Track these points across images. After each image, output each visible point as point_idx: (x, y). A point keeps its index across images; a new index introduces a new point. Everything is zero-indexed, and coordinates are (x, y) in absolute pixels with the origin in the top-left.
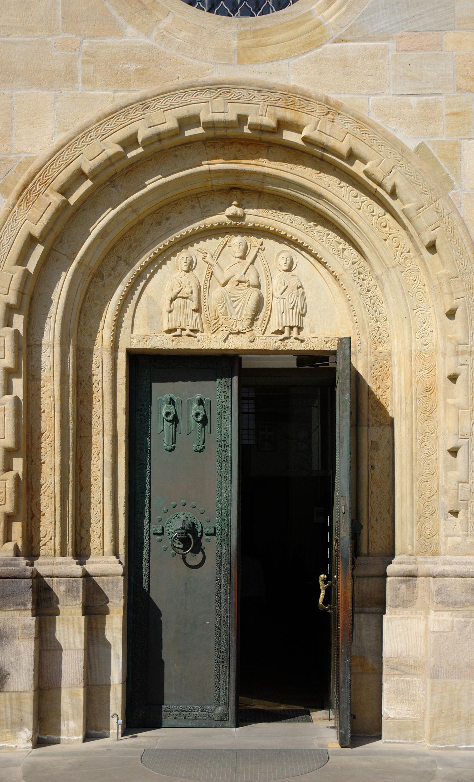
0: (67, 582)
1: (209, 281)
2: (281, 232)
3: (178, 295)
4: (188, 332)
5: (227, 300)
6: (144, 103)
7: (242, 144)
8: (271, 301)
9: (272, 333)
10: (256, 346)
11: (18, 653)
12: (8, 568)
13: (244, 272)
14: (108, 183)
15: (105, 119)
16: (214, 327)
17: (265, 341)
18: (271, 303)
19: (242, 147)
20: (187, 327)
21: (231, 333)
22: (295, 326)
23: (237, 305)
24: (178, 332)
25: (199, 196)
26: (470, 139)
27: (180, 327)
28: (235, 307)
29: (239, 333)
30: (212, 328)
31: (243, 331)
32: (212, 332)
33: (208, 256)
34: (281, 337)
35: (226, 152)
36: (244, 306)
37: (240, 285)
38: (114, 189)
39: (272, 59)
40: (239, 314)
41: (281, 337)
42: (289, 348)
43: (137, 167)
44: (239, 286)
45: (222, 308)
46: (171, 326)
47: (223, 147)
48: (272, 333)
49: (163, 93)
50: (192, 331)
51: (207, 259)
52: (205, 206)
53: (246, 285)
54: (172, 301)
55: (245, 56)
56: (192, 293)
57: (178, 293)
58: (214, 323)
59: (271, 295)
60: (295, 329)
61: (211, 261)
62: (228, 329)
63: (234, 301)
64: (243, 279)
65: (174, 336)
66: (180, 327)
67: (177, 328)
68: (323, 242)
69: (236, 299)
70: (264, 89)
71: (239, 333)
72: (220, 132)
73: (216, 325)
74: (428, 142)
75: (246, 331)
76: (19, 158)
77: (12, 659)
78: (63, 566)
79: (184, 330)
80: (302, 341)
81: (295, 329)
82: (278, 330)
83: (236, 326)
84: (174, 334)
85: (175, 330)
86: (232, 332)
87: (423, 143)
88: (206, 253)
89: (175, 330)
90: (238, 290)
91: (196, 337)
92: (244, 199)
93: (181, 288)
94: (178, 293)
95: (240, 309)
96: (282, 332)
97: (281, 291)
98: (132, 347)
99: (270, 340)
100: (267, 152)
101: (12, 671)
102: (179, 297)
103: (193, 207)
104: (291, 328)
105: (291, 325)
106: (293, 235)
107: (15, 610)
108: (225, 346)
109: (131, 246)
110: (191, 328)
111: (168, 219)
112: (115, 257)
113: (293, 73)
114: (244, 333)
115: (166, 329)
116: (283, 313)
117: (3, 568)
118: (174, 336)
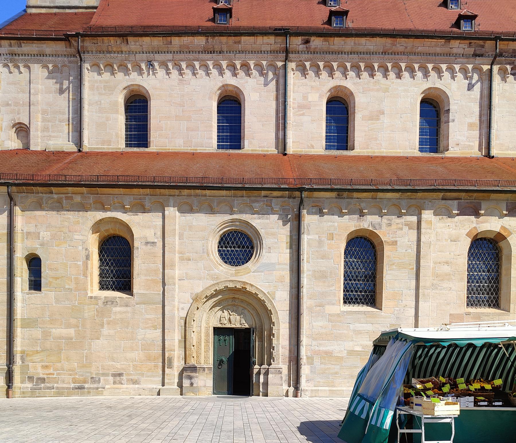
55: (236, 274)
70: (239, 282)
113: (245, 278)
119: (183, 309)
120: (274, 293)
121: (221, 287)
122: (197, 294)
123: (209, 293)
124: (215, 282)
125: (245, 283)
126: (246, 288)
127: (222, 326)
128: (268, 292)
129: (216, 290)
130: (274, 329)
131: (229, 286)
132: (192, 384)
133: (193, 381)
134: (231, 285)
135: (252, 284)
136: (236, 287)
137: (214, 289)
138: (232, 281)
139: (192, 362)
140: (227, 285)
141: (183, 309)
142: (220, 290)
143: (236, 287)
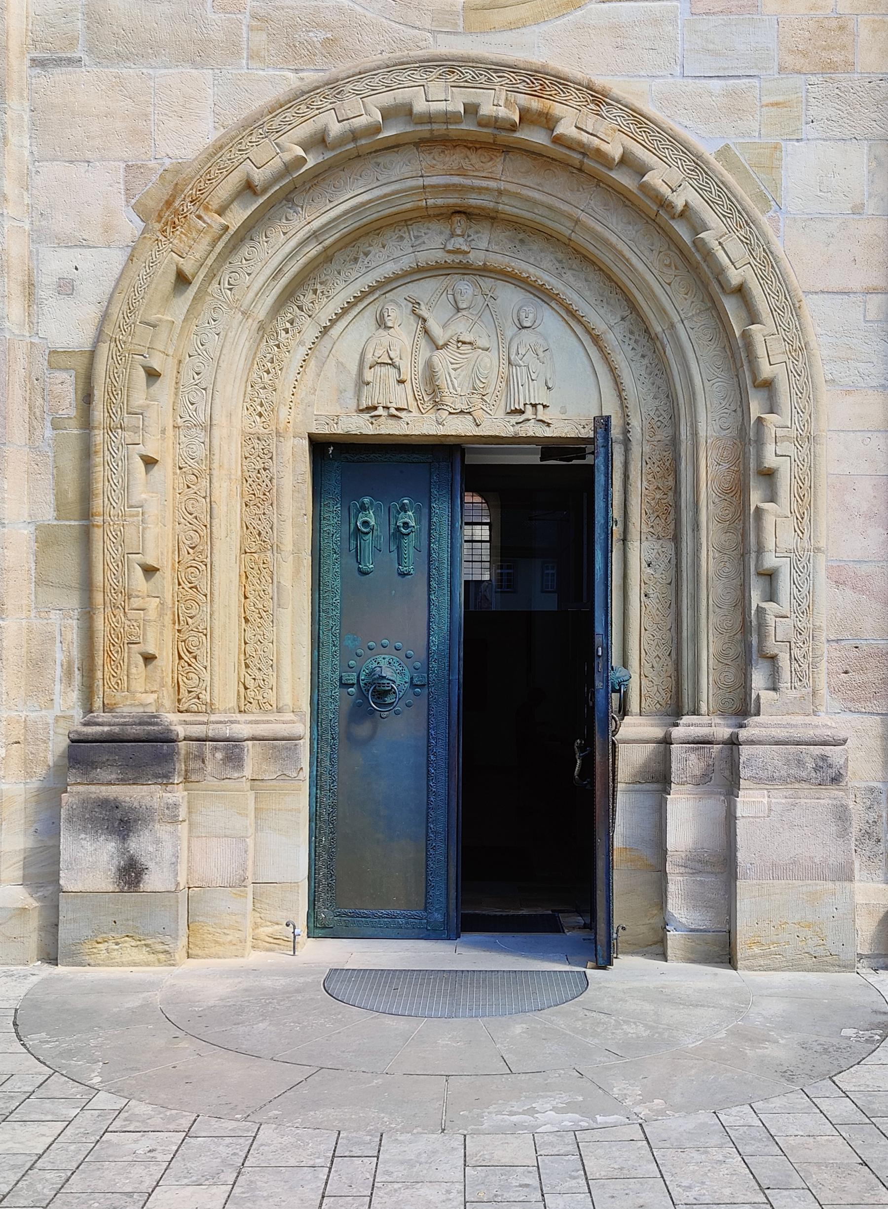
0: (226, 748)
6: (334, 87)
7: (469, 148)
10: (486, 430)
11: (158, 841)
12: (145, 727)
14: (284, 202)
15: (280, 110)
19: (469, 153)
20: (389, 405)
24: (380, 411)
25: (409, 223)
26: (798, 140)
35: (447, 159)
38: (292, 211)
39: (512, 26)
42: (531, 434)
43: (324, 179)
47: (443, 152)
49: (360, 73)
50: (397, 409)
52: (417, 237)
59: (506, 362)
60: (540, 407)
62: (446, 408)
69: (458, 366)
70: (499, 68)
72: (439, 128)
74: (734, 144)
76: (162, 165)
77: (151, 849)
78: (220, 726)
80: (548, 425)
81: (540, 407)
84: (372, 414)
87: (727, 146)
89: (375, 408)
92: (471, 227)
98: (317, 432)
100: (504, 160)
101: (151, 865)
103: (402, 238)
104: (534, 406)
107: (156, 783)
108: (442, 431)
109: (315, 292)
111: (366, 254)
112: (295, 307)
117: (138, 728)
118: (372, 417)
119: (66, 287)
120: (771, 160)
121: (363, 111)
122: (178, 169)
123: (265, 160)
124: (311, 77)
125: (542, 80)
126: (547, 121)
127: (370, 430)
128: (724, 153)
129: (319, 141)
130: (771, 431)
131: (420, 106)
132: (131, 873)
133: (141, 844)
134: (437, 97)
135: (600, 81)
136: (471, 109)
137: (305, 130)
138: (448, 66)
139: (142, 696)
140: (401, 95)
141: (66, 287)
142: (354, 135)
143: (471, 109)
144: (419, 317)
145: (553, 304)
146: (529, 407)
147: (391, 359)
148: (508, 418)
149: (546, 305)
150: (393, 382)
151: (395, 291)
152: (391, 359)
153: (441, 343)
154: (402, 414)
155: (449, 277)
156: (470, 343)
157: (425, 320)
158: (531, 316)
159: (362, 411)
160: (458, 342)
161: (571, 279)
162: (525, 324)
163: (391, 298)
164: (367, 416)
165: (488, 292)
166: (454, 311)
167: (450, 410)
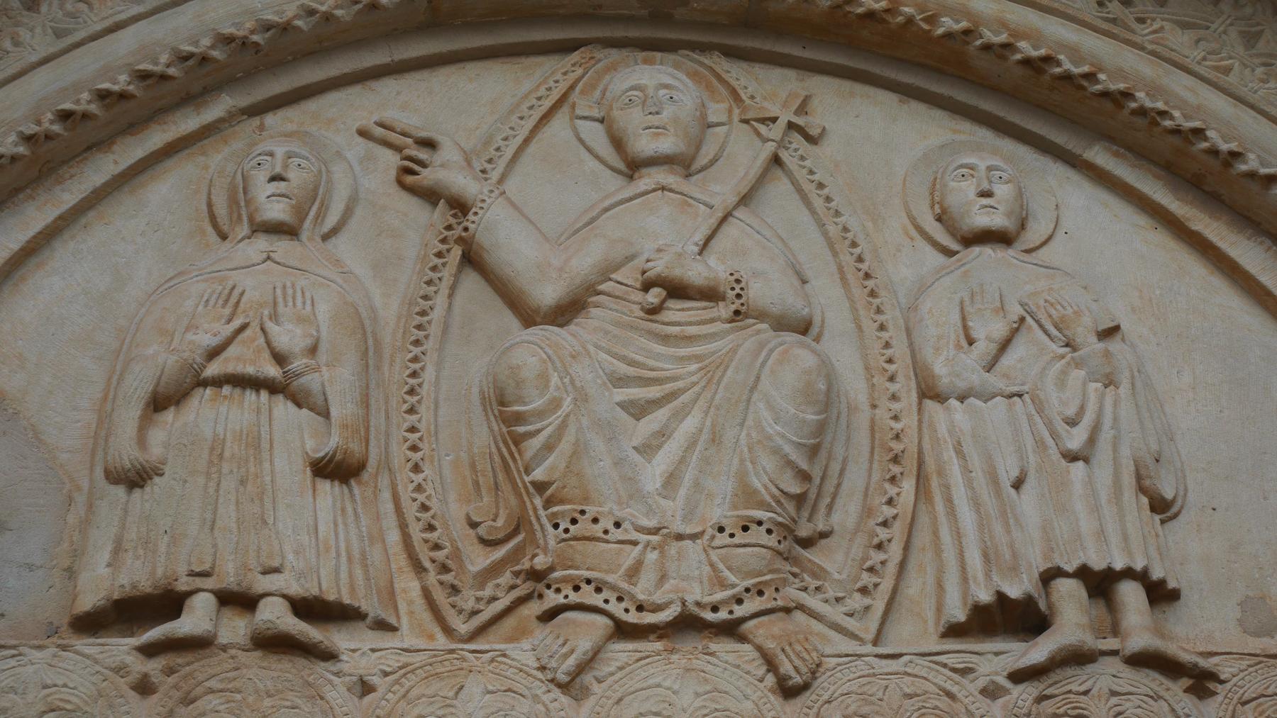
1: (440, 301)
2: (931, 20)
3: (213, 369)
4: (275, 615)
5: (582, 398)
8: (909, 422)
9: (954, 631)
13: (699, 237)
16: (488, 592)
17: (908, 685)
18: (912, 434)
20: (263, 584)
21: (623, 631)
22: (1129, 573)
23: (663, 435)
24: (197, 617)
27: (210, 583)
28: (647, 449)
29: (687, 624)
30: (467, 601)
31: (723, 615)
32: (463, 628)
33: (448, 152)
34: (1039, 651)
36: (715, 439)
37: (677, 311)
40: (682, 492)
41: (1039, 651)
44: (667, 316)
45: (549, 447)
46: (137, 576)
48: (954, 631)
51: (427, 177)
53: (724, 310)
54: (159, 402)
56: (313, 350)
57: (214, 353)
58: (474, 569)
59: (906, 388)
60: (1131, 595)
61: (461, 182)
62: (597, 600)
63: (638, 410)
64: (695, 273)
65: (149, 651)
66: (210, 583)
67: (183, 585)
68: (1227, 71)
69: (654, 392)
71: (687, 624)
73: (506, 578)
75: (740, 611)
79: (239, 600)
81: (1131, 595)
82: (1001, 596)
83: (663, 578)
85: (169, 603)
86: (633, 617)
88: (429, 144)
89: (169, 603)
90: (665, 339)
91: (329, 656)
93: (237, 323)
94: (214, 353)
95: (682, 461)
96: (1023, 618)
97: (984, 347)
99: (943, 679)
102: (218, 382)
104: (1100, 584)
105: (1098, 564)
106: (1017, 35)
110: (295, 589)
114: (731, 630)
115: (88, 601)
116: (1018, 485)
118: (149, 651)
144: (431, 196)
145: (1099, 156)
146: (1069, 594)
147: (280, 359)
148: (960, 652)
149: (1057, 171)
150: (287, 468)
151: (312, 105)
152: (280, 359)
153: (547, 294)
154: (340, 638)
155: (576, 56)
156: (710, 295)
157: (460, 207)
158: (1003, 191)
159: (91, 624)
160: (646, 287)
161: (1179, 41)
162: (982, 219)
163: (290, 127)
164: (120, 648)
165: (774, 110)
166: (613, 185)
167: (616, 608)
